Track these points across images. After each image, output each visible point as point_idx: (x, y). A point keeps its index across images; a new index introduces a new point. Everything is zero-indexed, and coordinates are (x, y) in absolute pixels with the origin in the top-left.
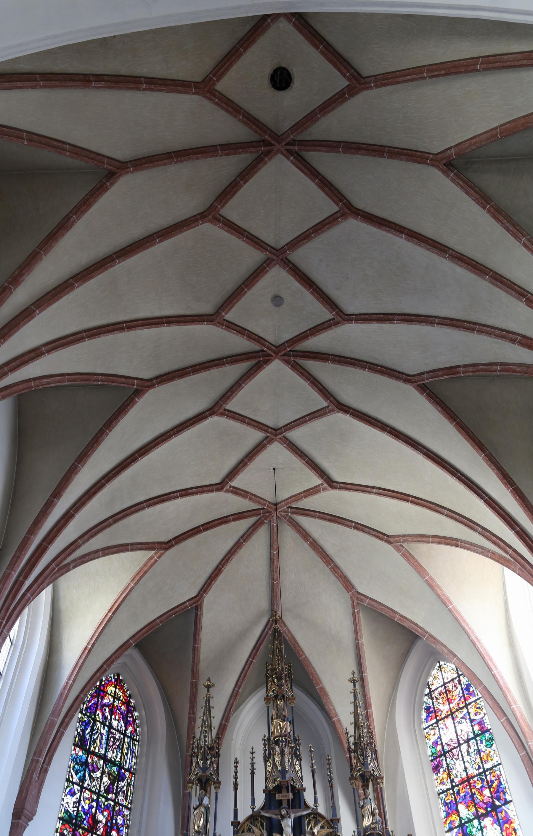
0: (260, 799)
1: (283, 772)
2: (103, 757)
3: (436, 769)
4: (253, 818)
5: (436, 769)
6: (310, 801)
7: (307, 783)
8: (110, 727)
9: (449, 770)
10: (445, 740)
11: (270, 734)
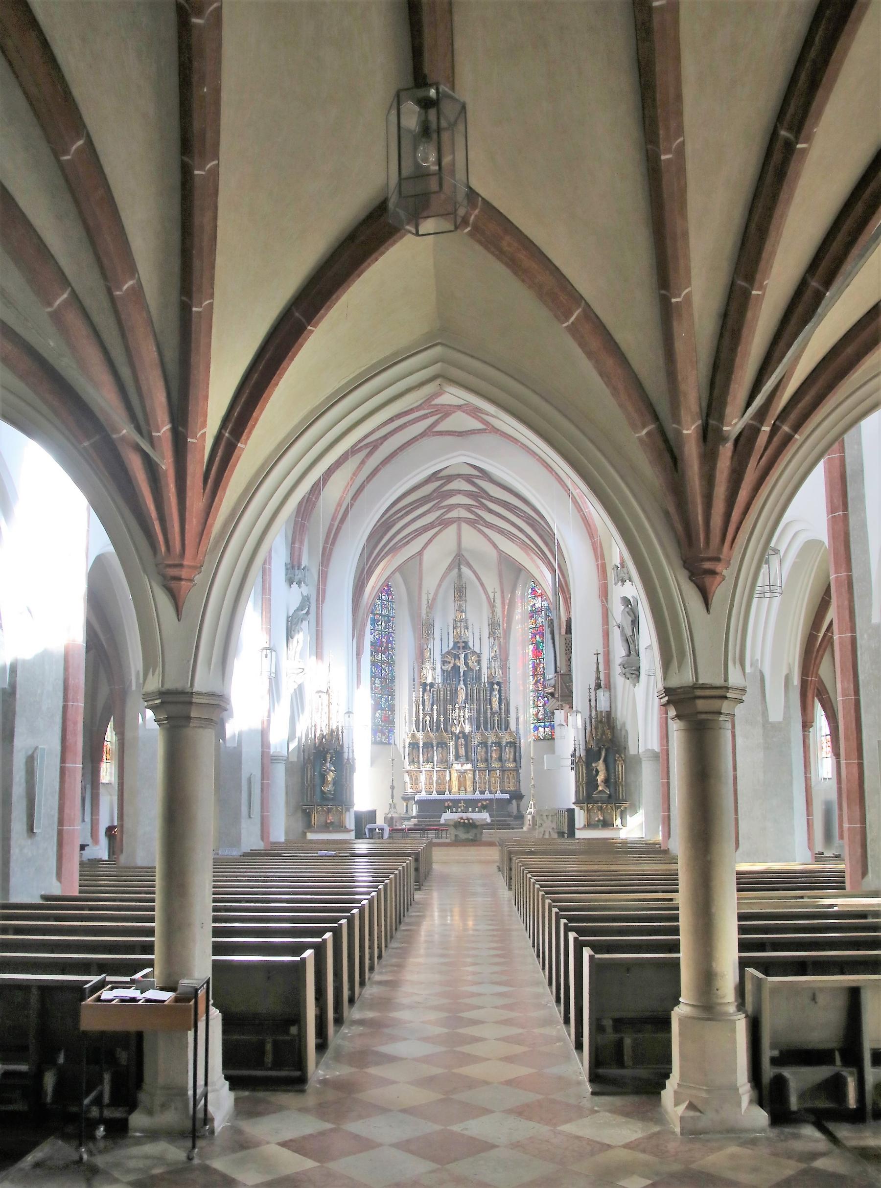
0: (451, 645)
1: (460, 637)
2: (381, 615)
3: (532, 617)
4: (448, 653)
5: (532, 617)
6: (471, 646)
7: (470, 639)
8: (382, 600)
9: (536, 620)
10: (537, 606)
11: (456, 617)
